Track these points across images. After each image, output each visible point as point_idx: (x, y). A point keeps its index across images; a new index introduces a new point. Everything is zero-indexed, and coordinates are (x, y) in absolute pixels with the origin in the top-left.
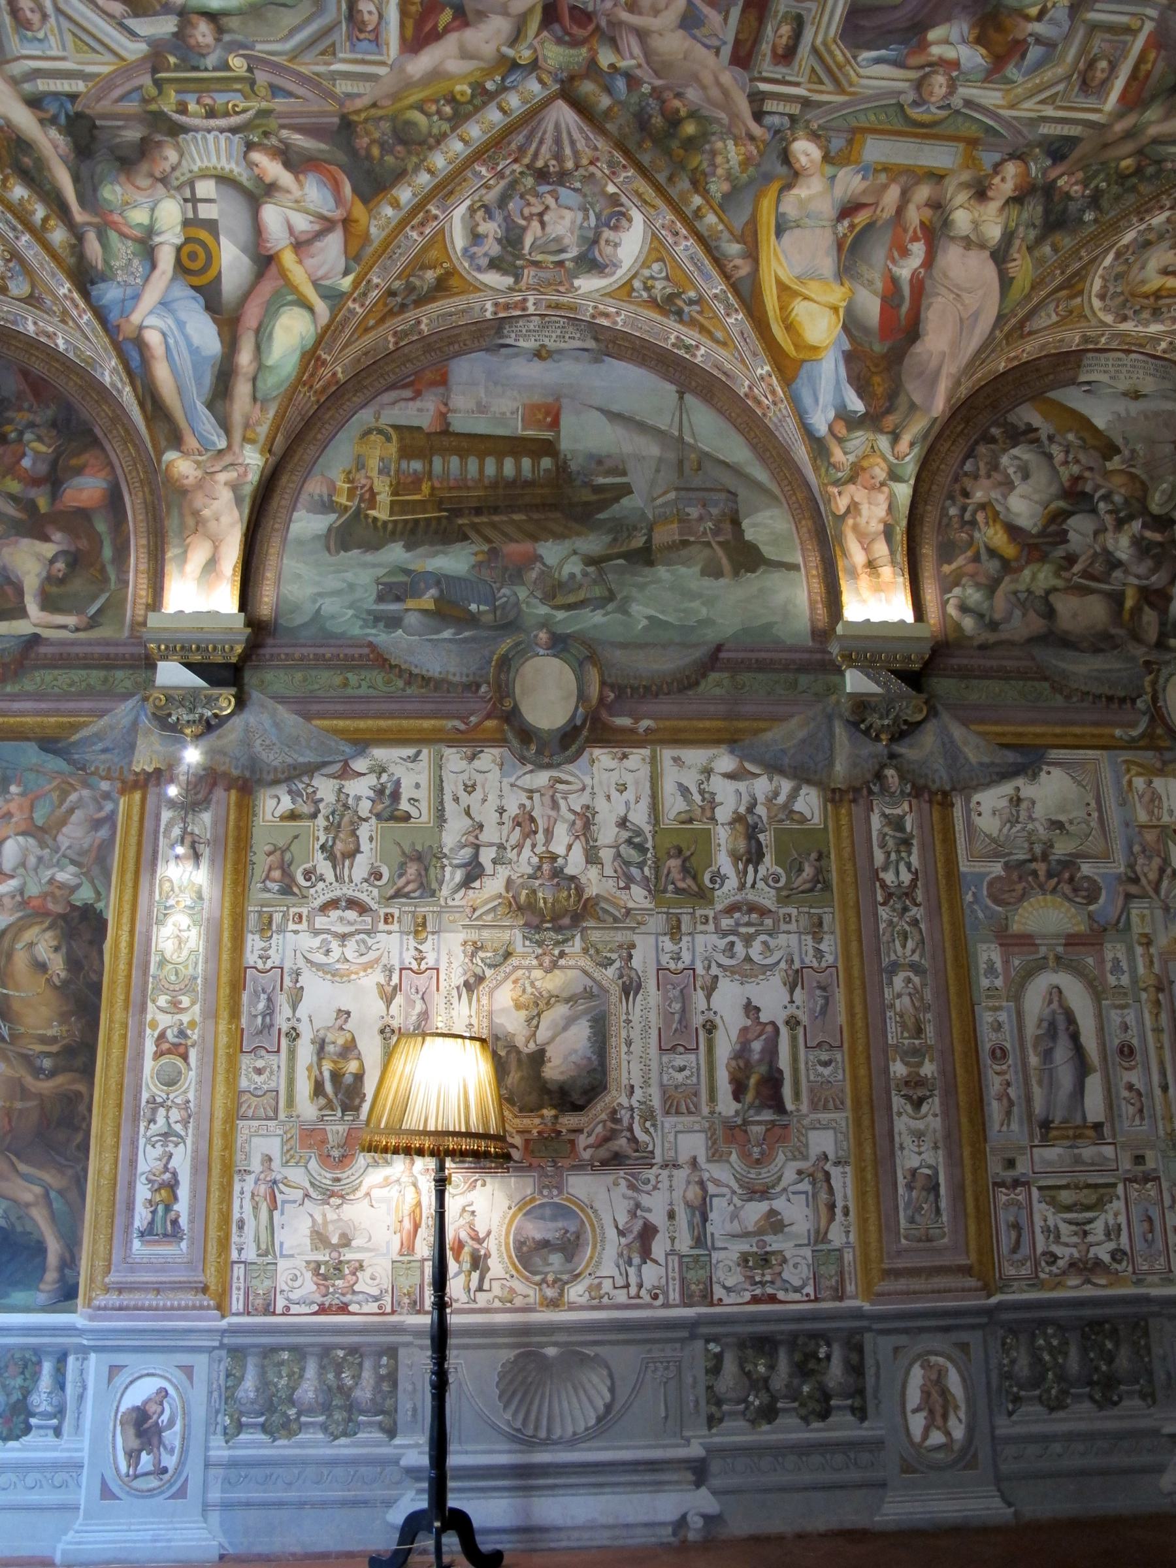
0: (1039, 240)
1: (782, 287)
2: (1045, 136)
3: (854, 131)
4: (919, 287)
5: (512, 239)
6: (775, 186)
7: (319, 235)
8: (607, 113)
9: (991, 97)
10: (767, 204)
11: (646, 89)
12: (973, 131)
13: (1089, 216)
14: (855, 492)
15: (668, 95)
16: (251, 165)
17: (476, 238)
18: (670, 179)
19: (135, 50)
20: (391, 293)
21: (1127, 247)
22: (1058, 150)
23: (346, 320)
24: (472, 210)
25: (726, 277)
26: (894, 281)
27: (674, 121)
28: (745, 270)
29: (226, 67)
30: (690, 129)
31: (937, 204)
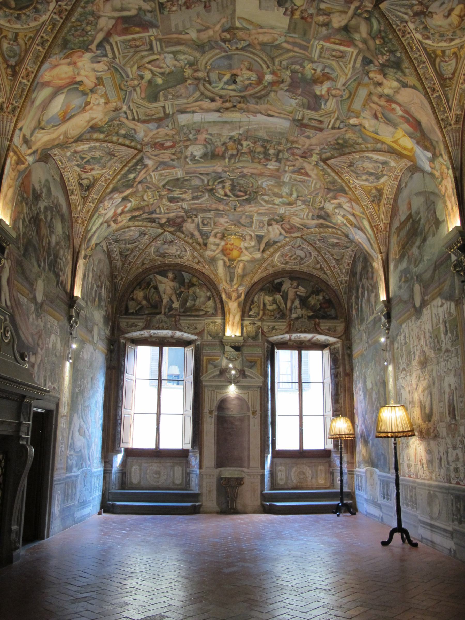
0: (403, 72)
1: (394, 142)
2: (361, 66)
3: (349, 110)
4: (406, 112)
5: (371, 174)
6: (363, 130)
7: (351, 204)
8: (332, 155)
9: (342, 80)
10: (368, 133)
11: (327, 147)
12: (355, 85)
13: (398, 54)
14: (445, 182)
15: (329, 144)
16: (333, 203)
17: (366, 180)
18: (355, 149)
19: (303, 206)
20: (373, 201)
21: (423, 35)
22: (367, 62)
23: (372, 215)
24: (357, 179)
25: (385, 152)
26: (402, 117)
27: (338, 144)
28: (386, 147)
29: (310, 198)
30: (341, 141)
31: (381, 96)
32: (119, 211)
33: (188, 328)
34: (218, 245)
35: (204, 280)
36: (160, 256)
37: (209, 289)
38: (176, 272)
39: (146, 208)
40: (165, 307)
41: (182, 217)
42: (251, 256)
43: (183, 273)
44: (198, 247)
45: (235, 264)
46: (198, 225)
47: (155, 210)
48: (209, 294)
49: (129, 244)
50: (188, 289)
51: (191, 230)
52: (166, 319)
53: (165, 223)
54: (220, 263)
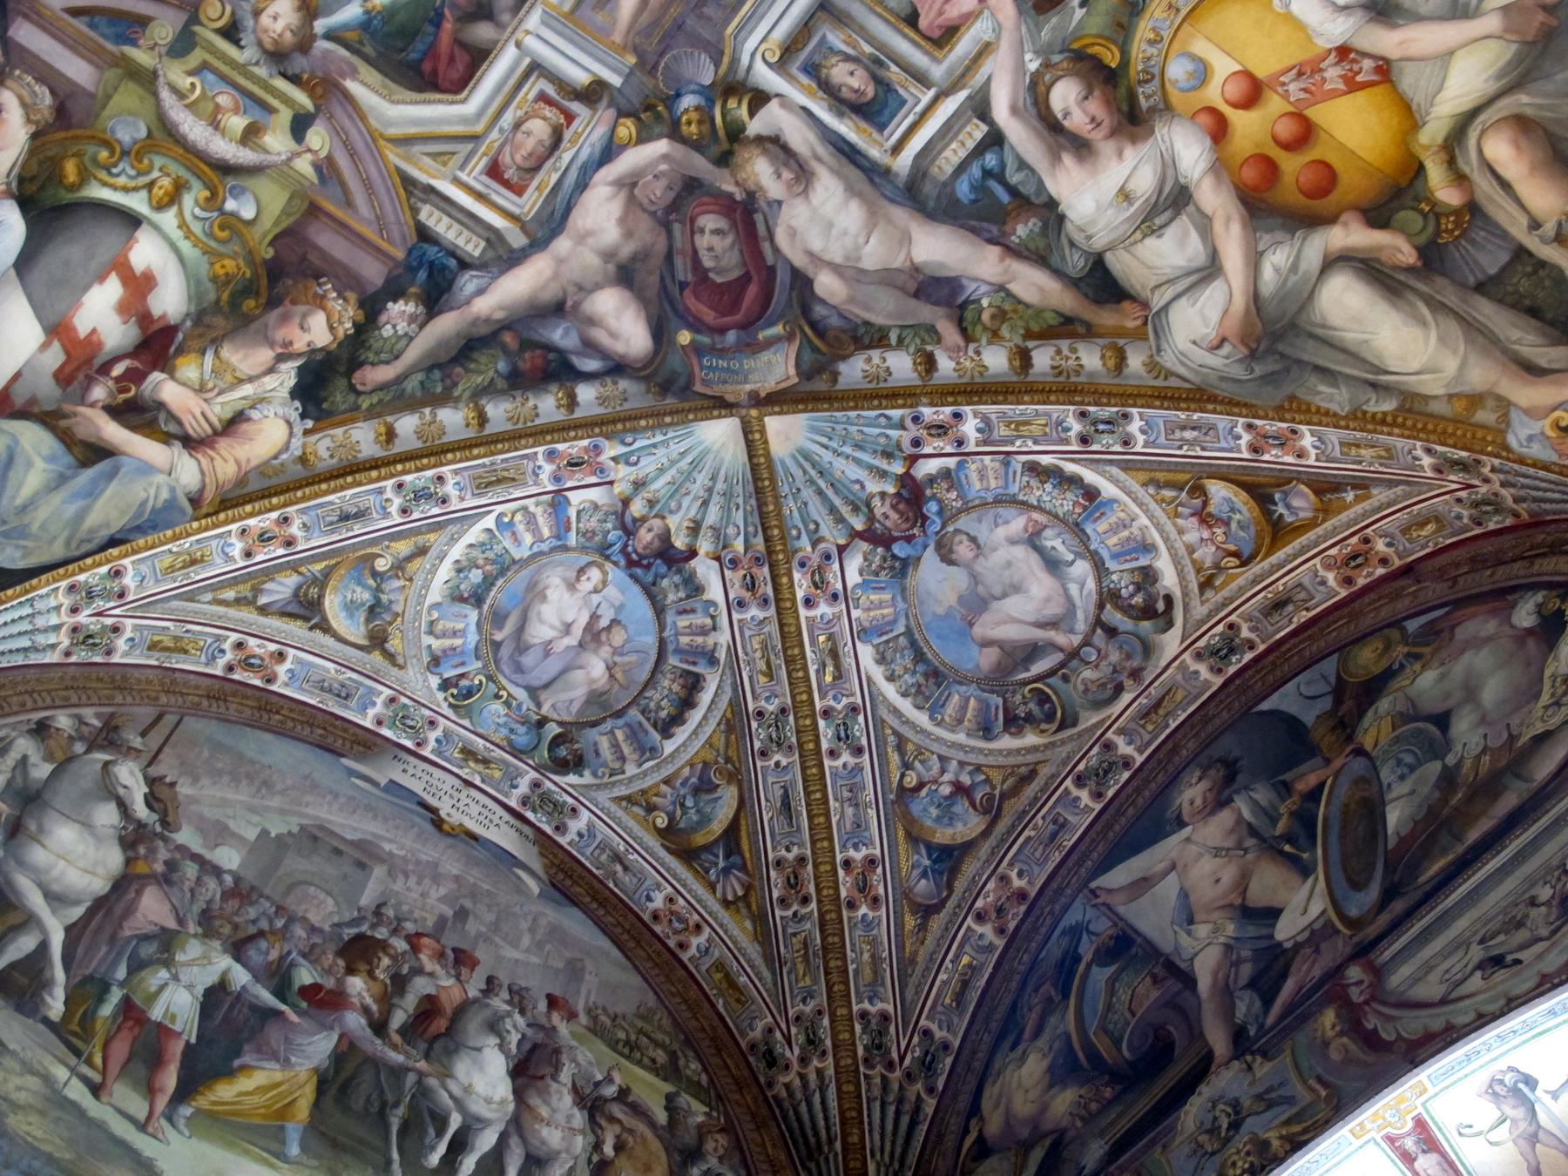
32: (100, 312)
33: (1497, 961)
34: (1176, 199)
35: (1434, 590)
36: (1013, 723)
37: (1502, 597)
38: (1229, 745)
39: (326, 240)
40: (1226, 993)
41: (691, 186)
42: (1491, 23)
43: (1265, 706)
44: (1091, 358)
45: (1449, 196)
46: (848, 152)
47: (424, 234)
48: (1525, 616)
49: (666, 733)
50: (1350, 739)
51: (874, 254)
52: (1263, 1069)
53: (659, 332)
54: (1346, 304)
